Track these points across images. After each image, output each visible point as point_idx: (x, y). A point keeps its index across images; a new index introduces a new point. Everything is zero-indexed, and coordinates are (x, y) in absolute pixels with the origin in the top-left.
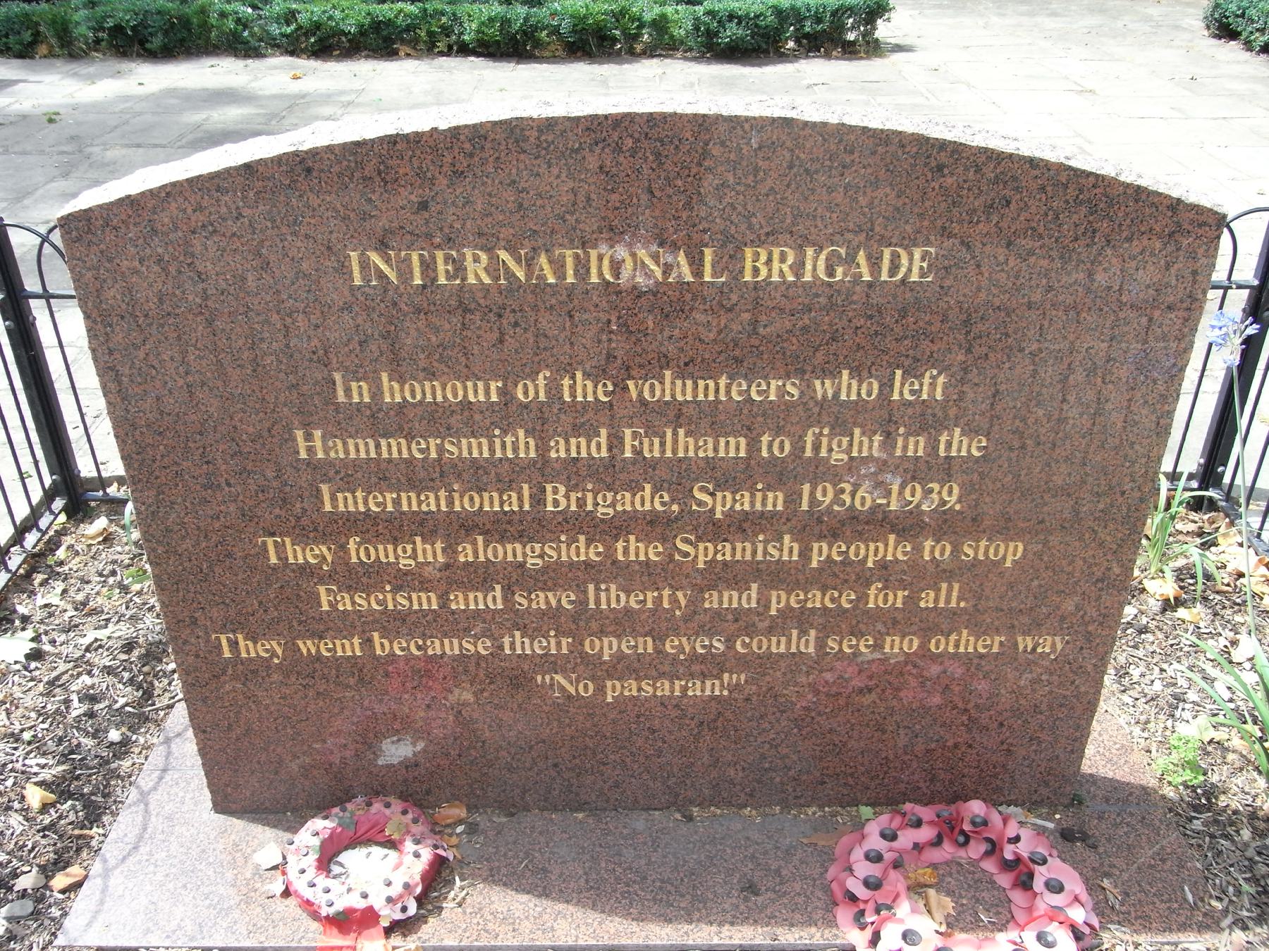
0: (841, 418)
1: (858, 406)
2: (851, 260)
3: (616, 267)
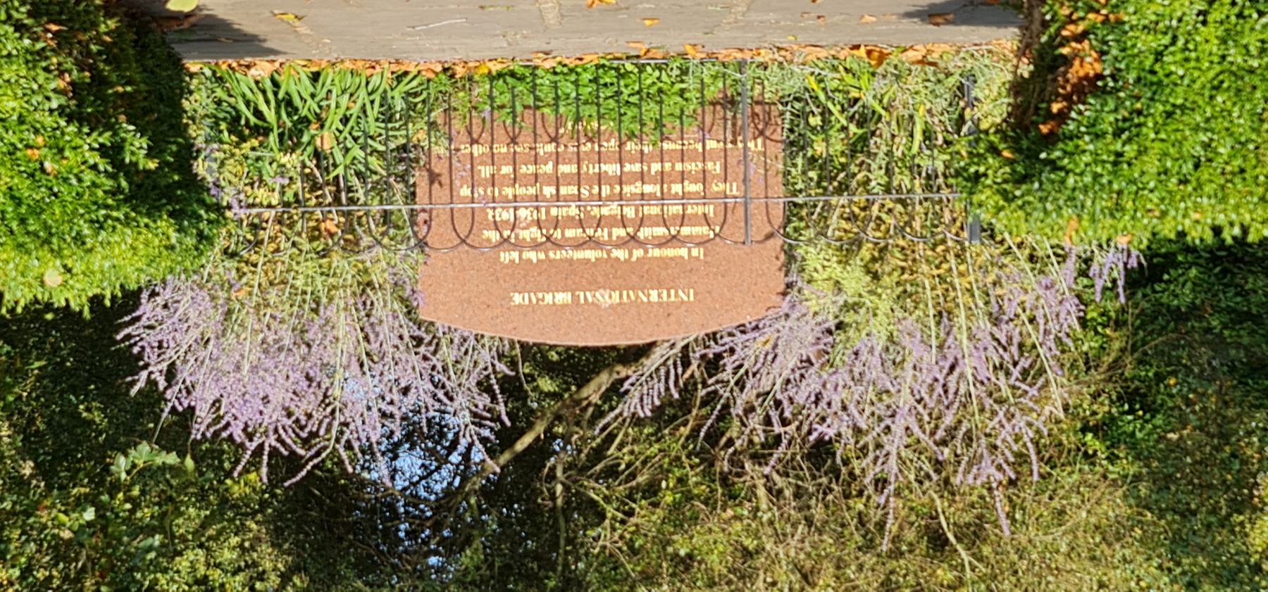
2: (538, 300)
3: (610, 297)
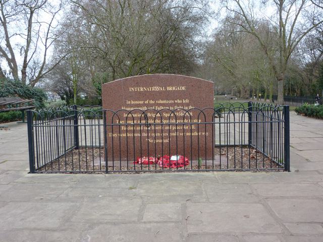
0: (178, 105)
1: (180, 103)
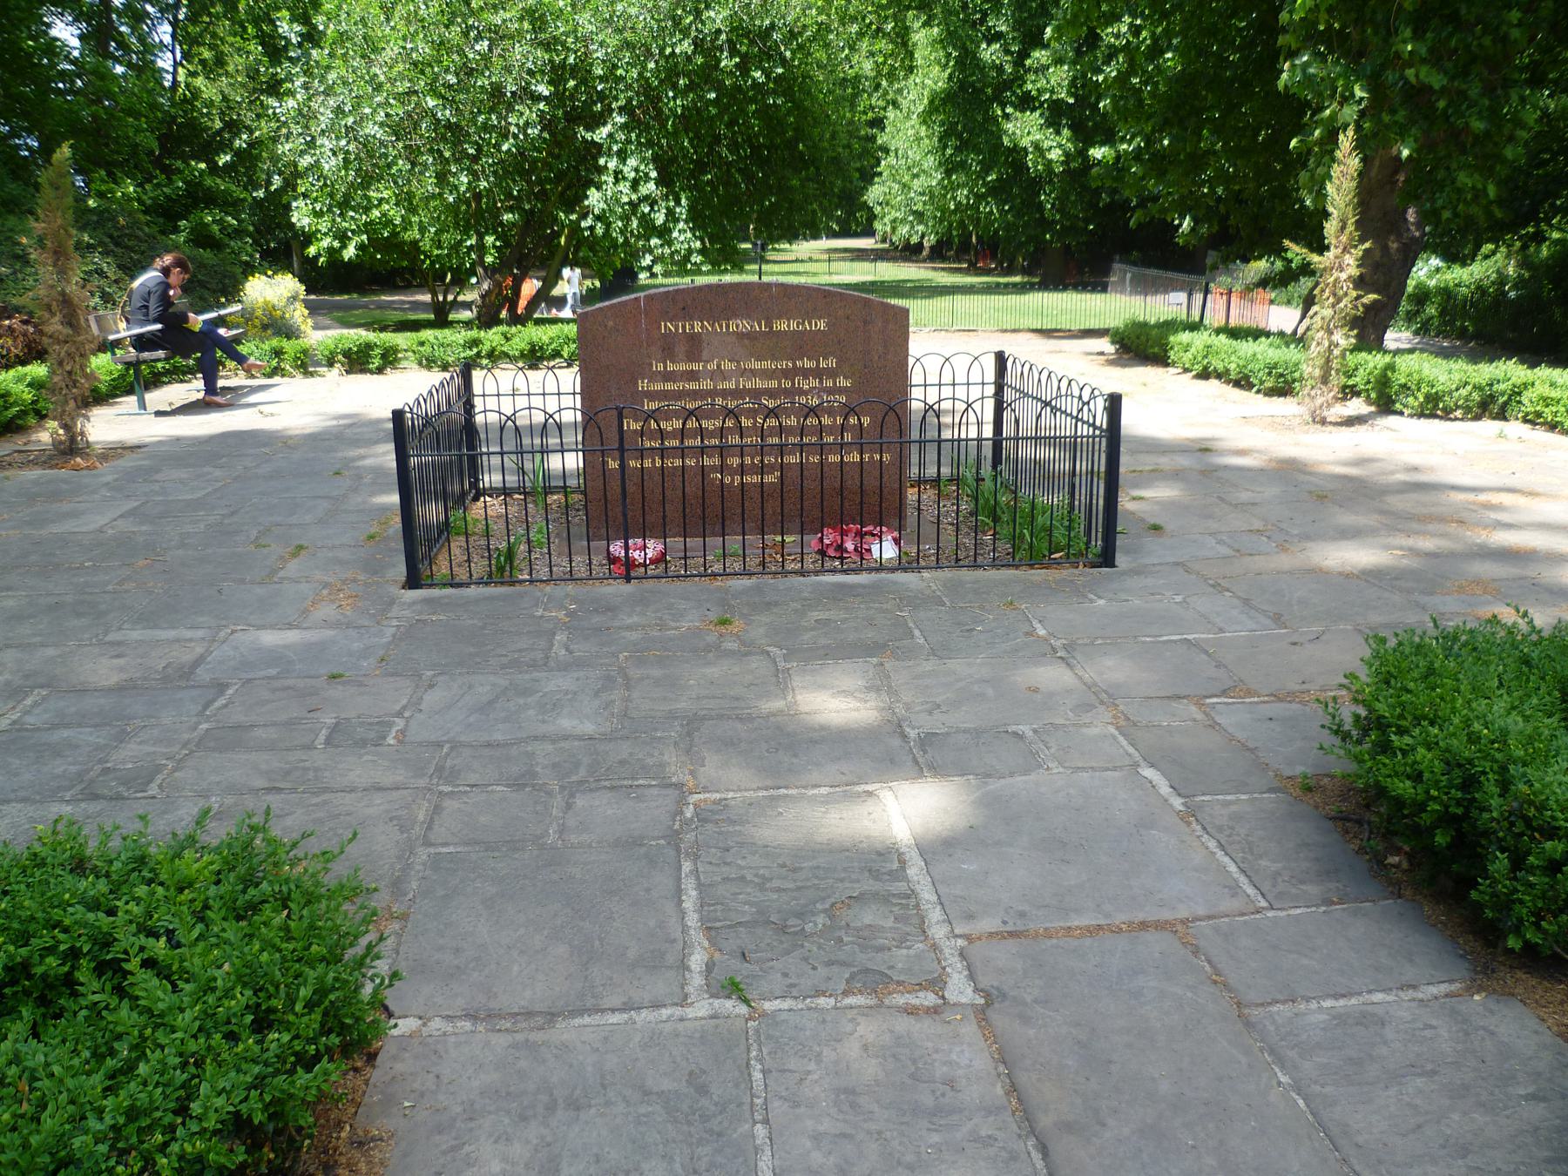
0: (806, 373)
